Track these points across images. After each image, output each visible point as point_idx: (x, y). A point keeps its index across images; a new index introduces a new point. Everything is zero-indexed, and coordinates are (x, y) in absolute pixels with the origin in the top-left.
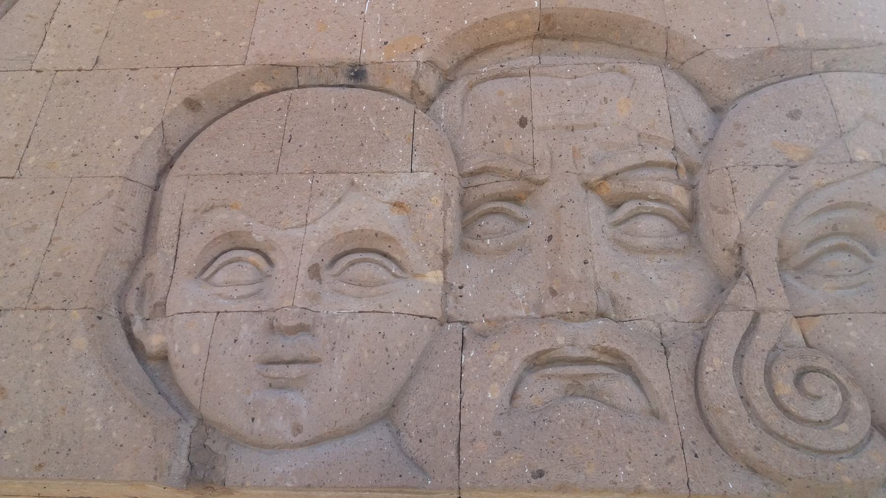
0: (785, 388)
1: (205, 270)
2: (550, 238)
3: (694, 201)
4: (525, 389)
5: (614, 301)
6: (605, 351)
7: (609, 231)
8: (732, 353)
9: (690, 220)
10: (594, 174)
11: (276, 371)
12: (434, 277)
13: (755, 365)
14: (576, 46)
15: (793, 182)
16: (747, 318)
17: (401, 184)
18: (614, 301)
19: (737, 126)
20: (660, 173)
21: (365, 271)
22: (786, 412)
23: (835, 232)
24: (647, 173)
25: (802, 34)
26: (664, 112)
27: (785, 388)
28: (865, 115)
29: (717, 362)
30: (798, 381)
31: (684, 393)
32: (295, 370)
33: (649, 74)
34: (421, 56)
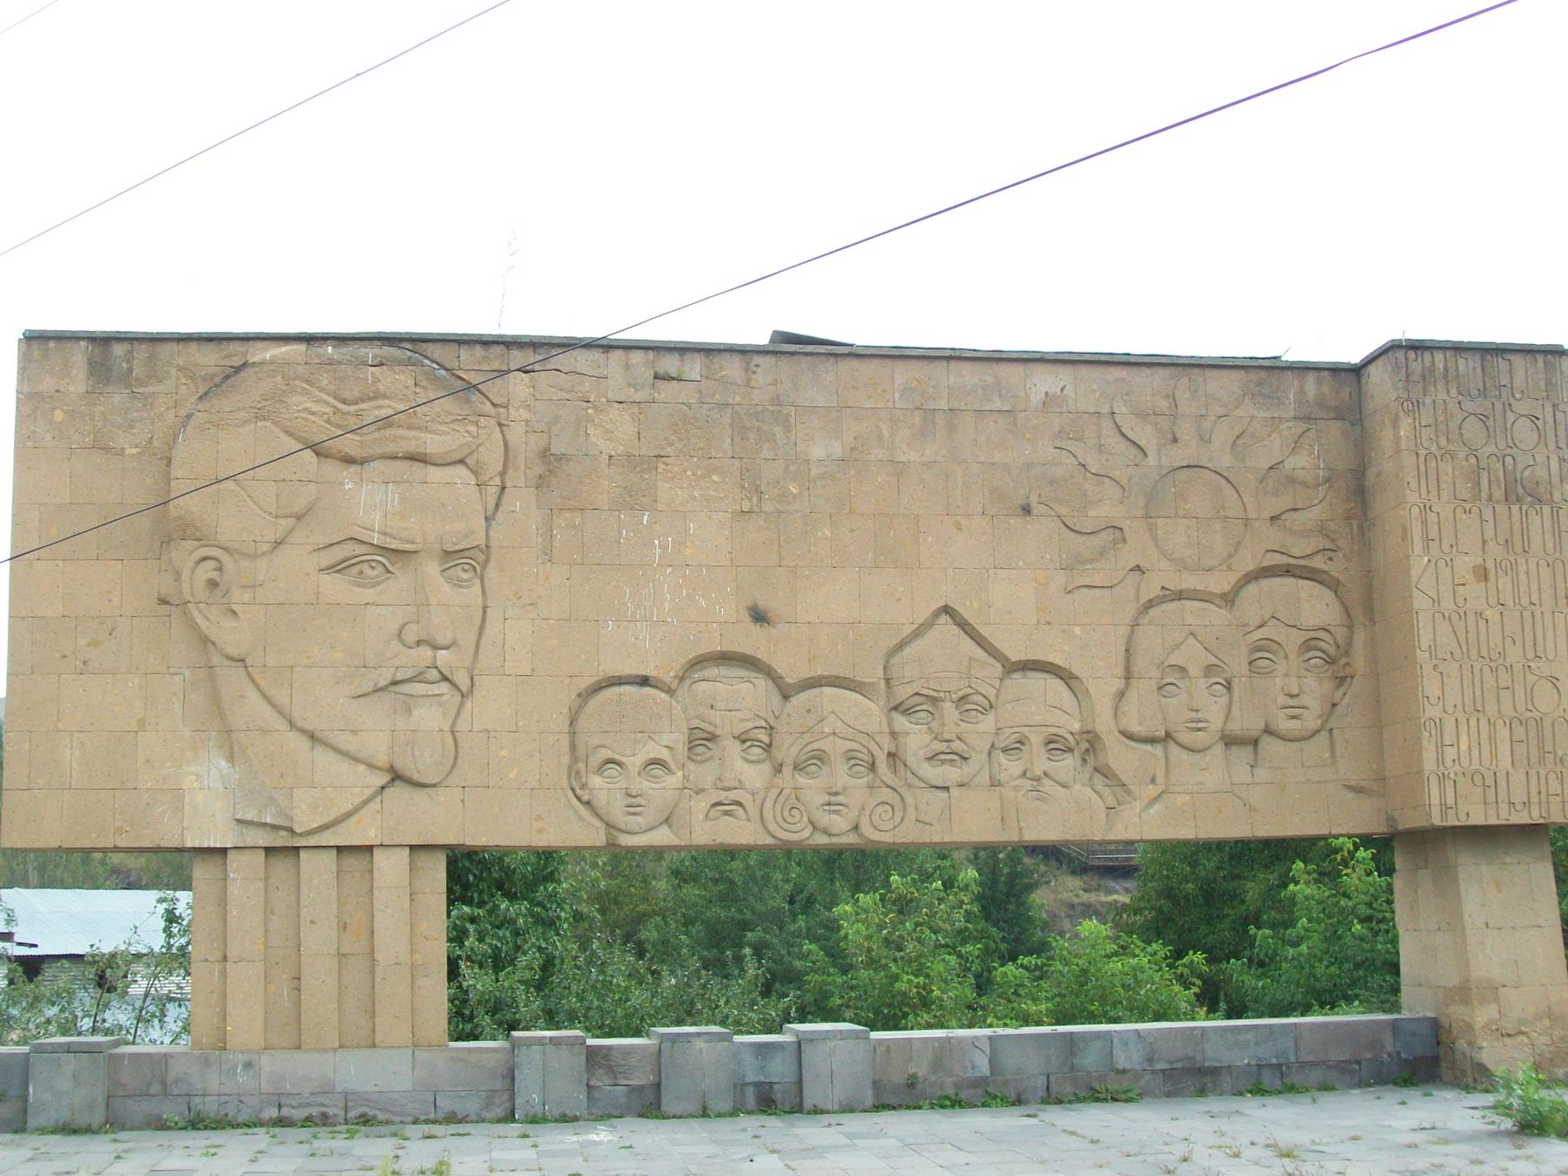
0: (786, 814)
1: (600, 770)
10: (737, 733)
11: (632, 810)
12: (680, 773)
17: (667, 738)
21: (657, 771)
27: (786, 814)
32: (638, 810)
33: (762, 683)
34: (672, 674)
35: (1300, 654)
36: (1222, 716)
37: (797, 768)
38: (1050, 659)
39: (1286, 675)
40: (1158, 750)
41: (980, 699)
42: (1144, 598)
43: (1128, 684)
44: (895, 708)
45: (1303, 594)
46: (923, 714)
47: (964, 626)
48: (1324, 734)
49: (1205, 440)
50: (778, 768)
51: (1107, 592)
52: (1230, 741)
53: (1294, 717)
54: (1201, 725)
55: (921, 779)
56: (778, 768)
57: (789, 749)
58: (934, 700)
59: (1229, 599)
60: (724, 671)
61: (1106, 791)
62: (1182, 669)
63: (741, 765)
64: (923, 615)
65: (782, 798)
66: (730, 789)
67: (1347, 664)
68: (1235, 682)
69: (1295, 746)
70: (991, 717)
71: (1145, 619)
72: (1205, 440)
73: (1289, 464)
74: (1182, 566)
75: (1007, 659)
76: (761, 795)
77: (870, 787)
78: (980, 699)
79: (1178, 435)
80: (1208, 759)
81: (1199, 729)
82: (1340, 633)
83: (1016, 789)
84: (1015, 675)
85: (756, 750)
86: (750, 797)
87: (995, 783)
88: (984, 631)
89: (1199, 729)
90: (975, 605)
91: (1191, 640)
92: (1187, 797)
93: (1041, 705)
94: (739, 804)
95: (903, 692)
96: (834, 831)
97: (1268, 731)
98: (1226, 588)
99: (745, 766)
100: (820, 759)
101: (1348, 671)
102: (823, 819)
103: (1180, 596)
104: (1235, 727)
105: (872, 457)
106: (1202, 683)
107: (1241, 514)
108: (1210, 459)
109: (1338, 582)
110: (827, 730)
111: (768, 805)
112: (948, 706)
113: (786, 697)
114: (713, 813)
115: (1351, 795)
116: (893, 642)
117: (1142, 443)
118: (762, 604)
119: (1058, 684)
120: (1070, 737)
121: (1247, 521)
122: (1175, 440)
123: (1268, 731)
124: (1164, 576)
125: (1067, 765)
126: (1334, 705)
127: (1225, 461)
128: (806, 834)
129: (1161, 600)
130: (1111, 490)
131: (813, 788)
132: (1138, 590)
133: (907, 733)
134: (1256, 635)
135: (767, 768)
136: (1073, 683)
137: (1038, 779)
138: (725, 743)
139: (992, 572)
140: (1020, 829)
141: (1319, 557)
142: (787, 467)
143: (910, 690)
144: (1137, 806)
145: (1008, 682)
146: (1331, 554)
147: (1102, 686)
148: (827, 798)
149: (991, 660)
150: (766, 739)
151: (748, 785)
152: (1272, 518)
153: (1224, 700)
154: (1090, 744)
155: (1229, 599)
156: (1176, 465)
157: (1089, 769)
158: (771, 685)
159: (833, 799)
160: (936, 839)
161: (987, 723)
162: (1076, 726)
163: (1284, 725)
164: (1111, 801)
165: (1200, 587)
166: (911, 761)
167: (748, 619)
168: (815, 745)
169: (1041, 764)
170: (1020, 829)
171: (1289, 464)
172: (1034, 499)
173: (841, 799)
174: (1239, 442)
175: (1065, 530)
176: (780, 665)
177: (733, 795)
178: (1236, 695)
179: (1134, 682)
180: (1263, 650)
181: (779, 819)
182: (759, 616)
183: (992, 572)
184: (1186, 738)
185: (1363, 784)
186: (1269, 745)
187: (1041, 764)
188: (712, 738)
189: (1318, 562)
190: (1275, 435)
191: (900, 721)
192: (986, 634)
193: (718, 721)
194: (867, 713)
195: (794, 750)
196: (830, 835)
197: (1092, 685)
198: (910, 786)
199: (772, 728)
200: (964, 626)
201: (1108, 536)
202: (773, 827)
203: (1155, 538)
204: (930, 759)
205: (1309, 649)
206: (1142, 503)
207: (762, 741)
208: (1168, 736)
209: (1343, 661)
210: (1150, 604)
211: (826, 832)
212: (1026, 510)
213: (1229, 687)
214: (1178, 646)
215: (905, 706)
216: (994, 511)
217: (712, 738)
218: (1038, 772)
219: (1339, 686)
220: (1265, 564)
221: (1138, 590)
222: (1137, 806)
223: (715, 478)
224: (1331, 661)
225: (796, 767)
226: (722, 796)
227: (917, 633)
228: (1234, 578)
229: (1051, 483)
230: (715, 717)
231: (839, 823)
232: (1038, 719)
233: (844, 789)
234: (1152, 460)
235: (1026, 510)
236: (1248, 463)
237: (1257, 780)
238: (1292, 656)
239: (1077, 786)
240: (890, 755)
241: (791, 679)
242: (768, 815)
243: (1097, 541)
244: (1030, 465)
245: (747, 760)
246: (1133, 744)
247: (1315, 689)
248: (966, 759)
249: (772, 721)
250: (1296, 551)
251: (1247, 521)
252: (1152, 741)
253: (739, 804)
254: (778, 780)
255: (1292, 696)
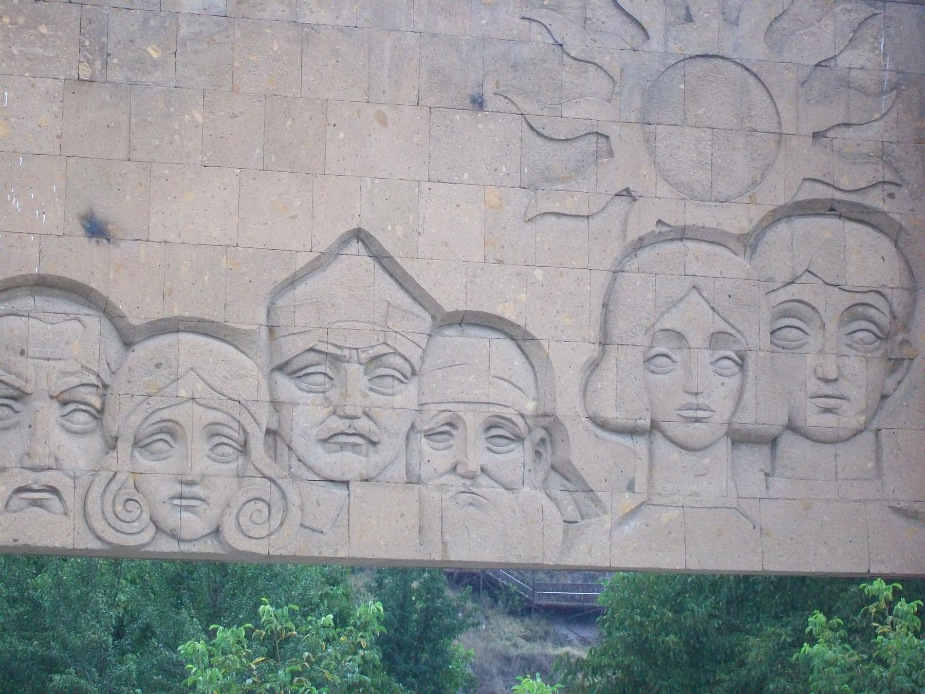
0: (119, 508)
2: (30, 426)
3: (103, 404)
4: (12, 503)
5: (57, 459)
6: (48, 486)
7: (60, 420)
8: (101, 490)
9: (99, 414)
10: (55, 391)
13: (109, 497)
14: (56, 291)
15: (148, 406)
16: (112, 474)
18: (57, 459)
19: (130, 369)
20: (89, 389)
22: (117, 517)
23: (161, 431)
24: (82, 389)
25: (176, 312)
26: (97, 352)
27: (119, 508)
28: (192, 369)
29: (94, 495)
30: (124, 506)
31: (79, 506)
33: (94, 323)
35: (842, 323)
36: (730, 404)
37: (138, 444)
38: (499, 311)
39: (821, 352)
40: (640, 445)
41: (398, 361)
42: (633, 236)
43: (603, 352)
44: (281, 368)
45: (851, 242)
46: (319, 379)
47: (382, 258)
48: (868, 436)
49: (731, 21)
50: (112, 444)
51: (582, 224)
52: (740, 438)
53: (828, 410)
54: (700, 414)
55: (310, 468)
56: (112, 444)
57: (128, 418)
58: (335, 360)
59: (749, 243)
60: (41, 302)
61: (565, 499)
62: (680, 336)
63: (58, 436)
64: (326, 239)
65: (114, 486)
66: (42, 469)
67: (905, 342)
68: (751, 359)
69: (829, 450)
70: (412, 389)
71: (632, 265)
72: (731, 21)
73: (844, 61)
74: (688, 193)
75: (439, 307)
76: (85, 480)
77: (240, 476)
78: (398, 361)
79: (694, 10)
80: (706, 461)
81: (698, 420)
82: (899, 298)
83: (442, 488)
84: (450, 332)
85: (81, 417)
86: (69, 482)
87: (413, 479)
88: (411, 268)
89: (698, 420)
90: (400, 231)
91: (694, 296)
92: (675, 513)
93: (485, 375)
94: (54, 490)
95: (292, 346)
96: (185, 534)
97: (792, 427)
98: (747, 227)
99: (65, 439)
100: (171, 433)
101: (906, 351)
102: (171, 517)
103: (682, 234)
104: (747, 419)
105: (267, 15)
106: (706, 356)
107: (773, 127)
108: (735, 50)
109: (901, 228)
110: (183, 393)
111: (95, 494)
112: (354, 369)
113: (128, 344)
114: (16, 502)
115: (897, 521)
116: (282, 276)
117: (644, 20)
118: (104, 210)
119: (508, 346)
120: (520, 422)
121: (780, 136)
122: (689, 19)
123: (792, 427)
124: (661, 206)
125: (513, 460)
126: (884, 397)
127: (756, 50)
128: (146, 537)
129: (657, 239)
130: (598, 83)
131: (159, 474)
132: (625, 223)
133: (295, 404)
134: (783, 295)
135: (95, 442)
136: (527, 345)
137: (473, 477)
138: (37, 404)
139: (425, 186)
140: (445, 544)
141: (877, 192)
142: (146, 20)
143: (302, 343)
144: (607, 521)
145: (439, 339)
146: (892, 189)
147: (569, 354)
148: (178, 488)
149: (417, 309)
150: (96, 402)
151: (67, 464)
152: (817, 135)
153: (734, 382)
154: (547, 431)
155: (749, 243)
156: (688, 53)
157: (544, 466)
158: (106, 324)
159: (186, 490)
160: (328, 553)
161: (407, 395)
162: (530, 407)
163: (813, 420)
164: (571, 512)
165: (710, 223)
166: (299, 444)
167: (80, 231)
168: (165, 414)
169: (478, 455)
170: (445, 544)
171: (844, 61)
172: (489, 90)
173: (197, 490)
174: (777, 25)
175: (530, 133)
176: (121, 299)
177: (46, 478)
178: (751, 374)
179: (612, 350)
180: (791, 317)
181: (110, 515)
182: (96, 229)
183: (425, 186)
184: (679, 430)
185: (917, 506)
186: (794, 449)
187: (478, 455)
188: (20, 396)
189: (874, 200)
190: (828, 21)
191: (286, 387)
192: (412, 273)
193: (30, 372)
194: (237, 373)
195: (136, 419)
196: (180, 540)
197: (554, 351)
198: (294, 477)
199: (105, 386)
200: (382, 258)
201: (588, 145)
202: (100, 526)
203: (652, 152)
204: (325, 441)
205: (854, 318)
206: (637, 101)
207: (90, 405)
208: (655, 426)
209: (900, 337)
210: (641, 243)
211: (175, 536)
212: (478, 103)
213: (742, 364)
214: (675, 303)
215: (294, 366)
216: (432, 101)
217: (20, 396)
218: (473, 466)
219: (893, 371)
220: (802, 196)
221: (625, 223)
222: (607, 521)
223: (43, 29)
224: (883, 336)
225: (136, 443)
226: (29, 479)
227: (316, 266)
228: (757, 213)
229: (514, 66)
230: (27, 367)
231: (194, 524)
232: (477, 393)
233: (204, 476)
234: (655, 44)
235: (478, 103)
236: (787, 57)
237: (772, 493)
238: (831, 326)
239: (526, 489)
240: (269, 432)
241: (136, 319)
242: (94, 509)
243: (573, 152)
244: (485, 41)
245: (68, 430)
246: (606, 435)
247: (859, 374)
248: (374, 444)
249: (107, 380)
250: (845, 182)
251: (780, 136)
252: (632, 432)
253: (54, 490)
254: (111, 461)
255: (827, 381)
